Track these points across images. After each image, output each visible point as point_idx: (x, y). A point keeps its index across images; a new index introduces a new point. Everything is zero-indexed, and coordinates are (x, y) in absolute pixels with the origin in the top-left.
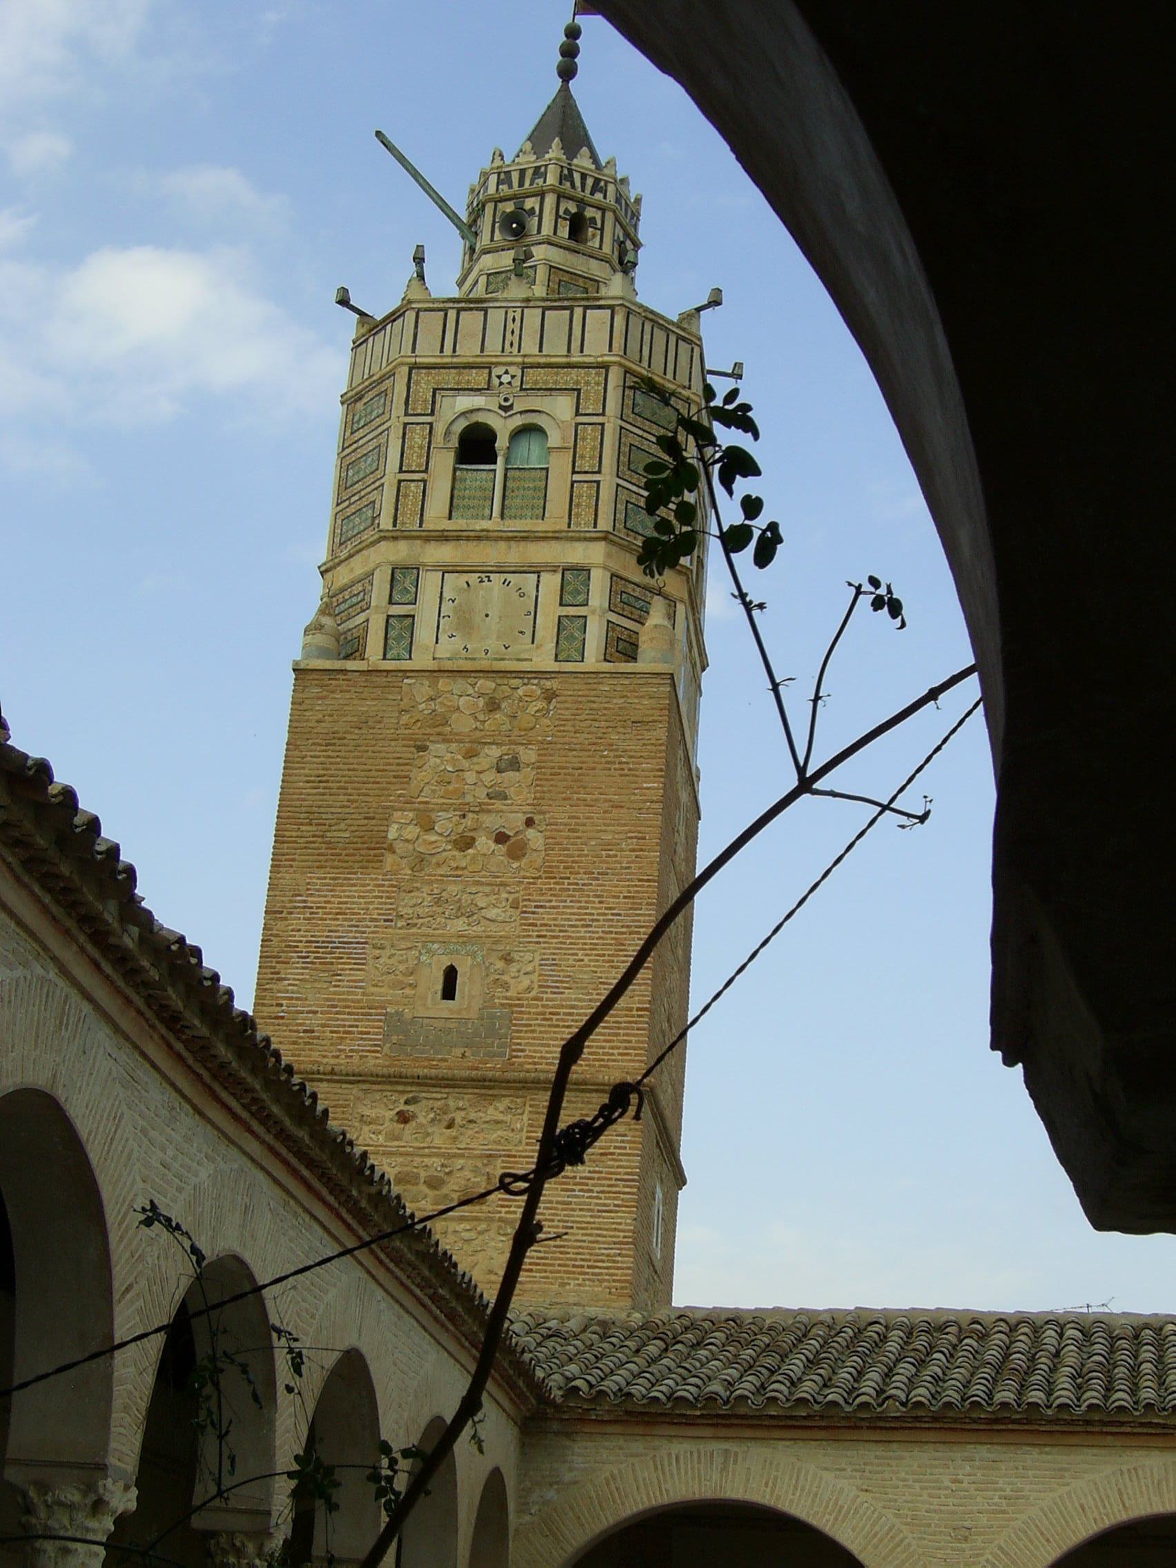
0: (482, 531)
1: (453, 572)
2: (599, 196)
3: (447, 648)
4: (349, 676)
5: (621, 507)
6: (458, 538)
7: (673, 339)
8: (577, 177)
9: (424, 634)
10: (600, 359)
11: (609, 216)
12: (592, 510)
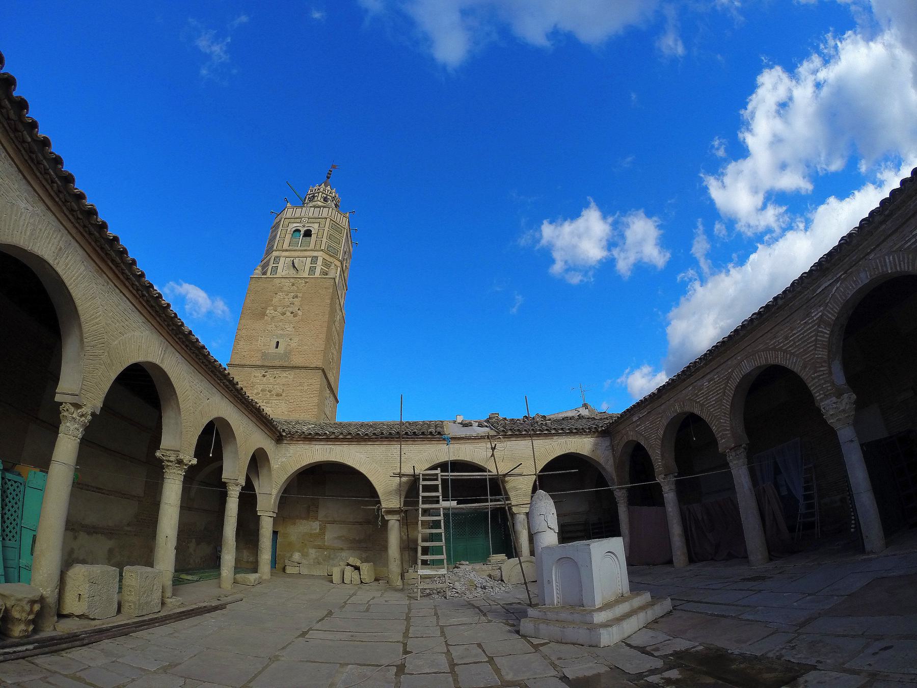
3: (284, 274)
9: (279, 270)
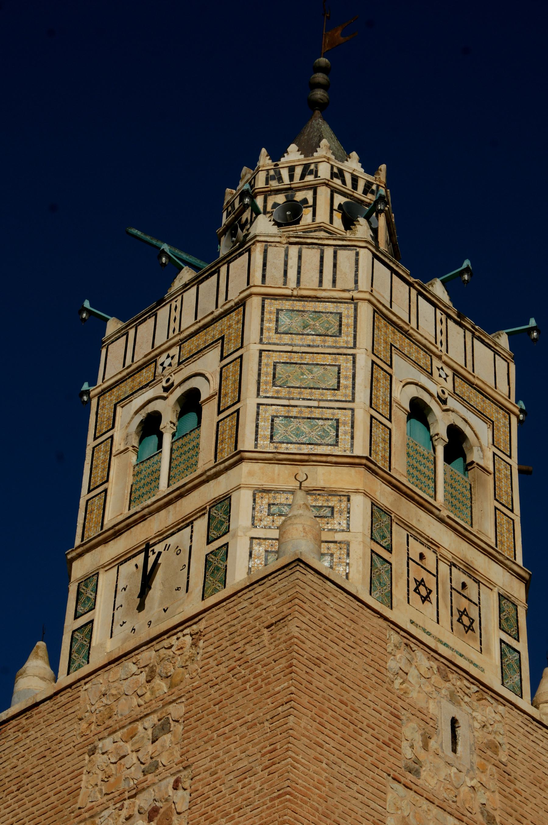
0: (143, 509)
1: (125, 561)
2: (309, 178)
4: (42, 707)
5: (265, 425)
6: (129, 527)
7: (329, 253)
8: (285, 174)
10: (236, 300)
11: (324, 193)
12: (233, 440)
